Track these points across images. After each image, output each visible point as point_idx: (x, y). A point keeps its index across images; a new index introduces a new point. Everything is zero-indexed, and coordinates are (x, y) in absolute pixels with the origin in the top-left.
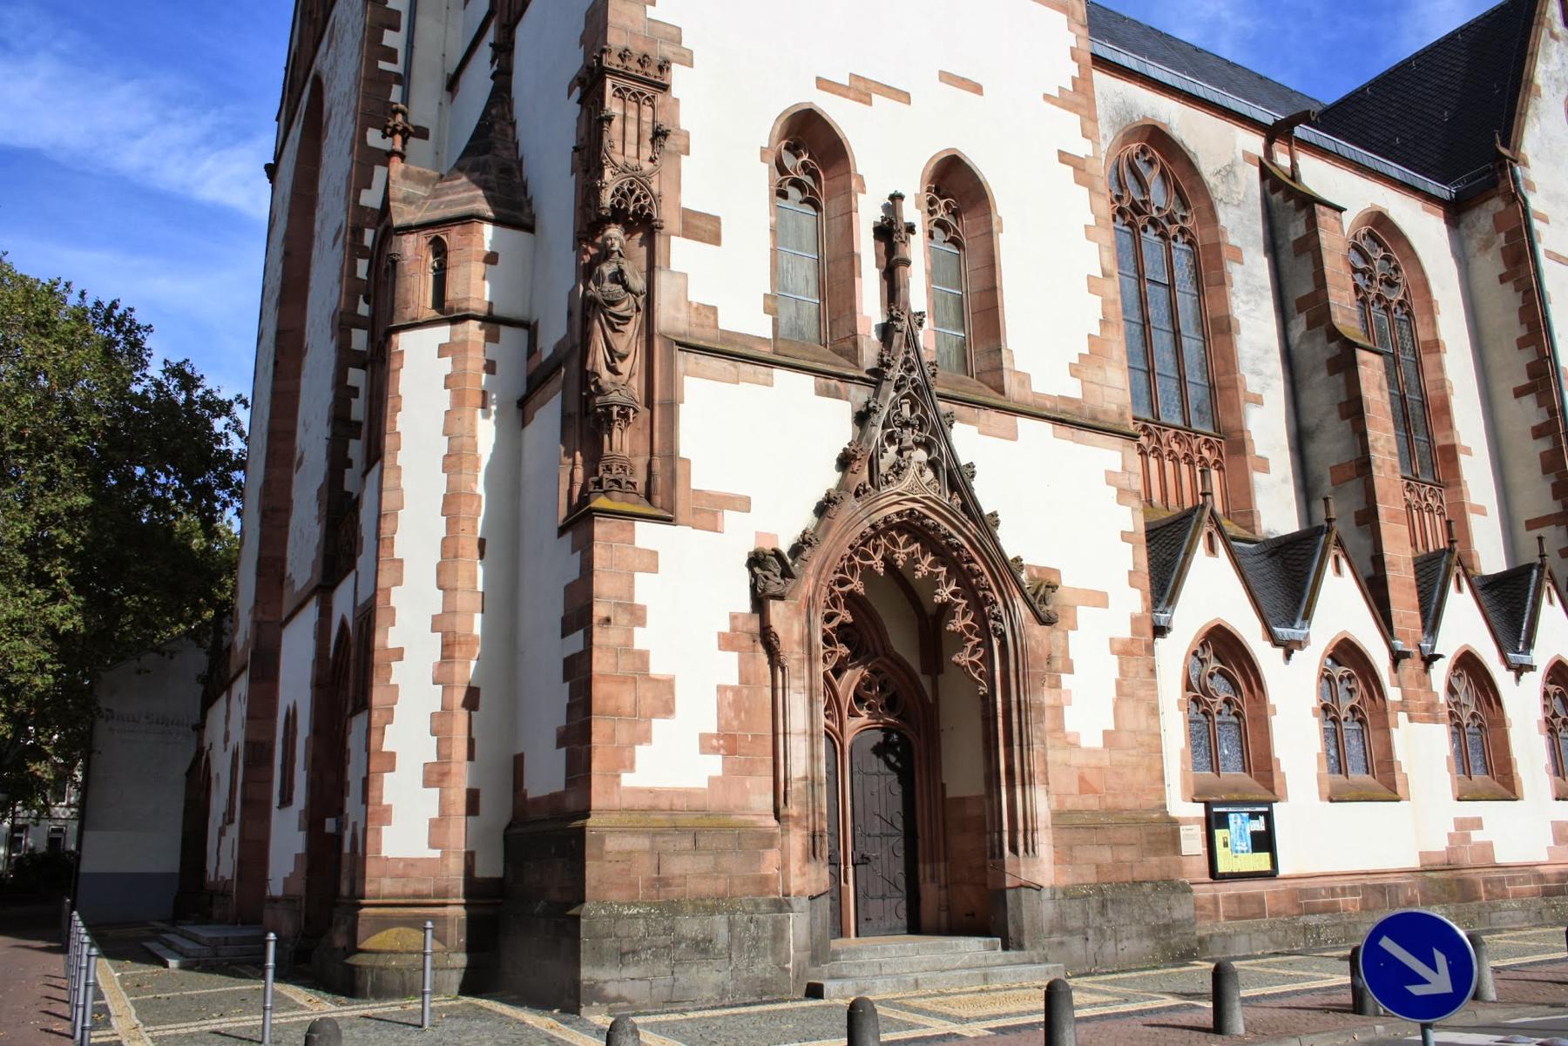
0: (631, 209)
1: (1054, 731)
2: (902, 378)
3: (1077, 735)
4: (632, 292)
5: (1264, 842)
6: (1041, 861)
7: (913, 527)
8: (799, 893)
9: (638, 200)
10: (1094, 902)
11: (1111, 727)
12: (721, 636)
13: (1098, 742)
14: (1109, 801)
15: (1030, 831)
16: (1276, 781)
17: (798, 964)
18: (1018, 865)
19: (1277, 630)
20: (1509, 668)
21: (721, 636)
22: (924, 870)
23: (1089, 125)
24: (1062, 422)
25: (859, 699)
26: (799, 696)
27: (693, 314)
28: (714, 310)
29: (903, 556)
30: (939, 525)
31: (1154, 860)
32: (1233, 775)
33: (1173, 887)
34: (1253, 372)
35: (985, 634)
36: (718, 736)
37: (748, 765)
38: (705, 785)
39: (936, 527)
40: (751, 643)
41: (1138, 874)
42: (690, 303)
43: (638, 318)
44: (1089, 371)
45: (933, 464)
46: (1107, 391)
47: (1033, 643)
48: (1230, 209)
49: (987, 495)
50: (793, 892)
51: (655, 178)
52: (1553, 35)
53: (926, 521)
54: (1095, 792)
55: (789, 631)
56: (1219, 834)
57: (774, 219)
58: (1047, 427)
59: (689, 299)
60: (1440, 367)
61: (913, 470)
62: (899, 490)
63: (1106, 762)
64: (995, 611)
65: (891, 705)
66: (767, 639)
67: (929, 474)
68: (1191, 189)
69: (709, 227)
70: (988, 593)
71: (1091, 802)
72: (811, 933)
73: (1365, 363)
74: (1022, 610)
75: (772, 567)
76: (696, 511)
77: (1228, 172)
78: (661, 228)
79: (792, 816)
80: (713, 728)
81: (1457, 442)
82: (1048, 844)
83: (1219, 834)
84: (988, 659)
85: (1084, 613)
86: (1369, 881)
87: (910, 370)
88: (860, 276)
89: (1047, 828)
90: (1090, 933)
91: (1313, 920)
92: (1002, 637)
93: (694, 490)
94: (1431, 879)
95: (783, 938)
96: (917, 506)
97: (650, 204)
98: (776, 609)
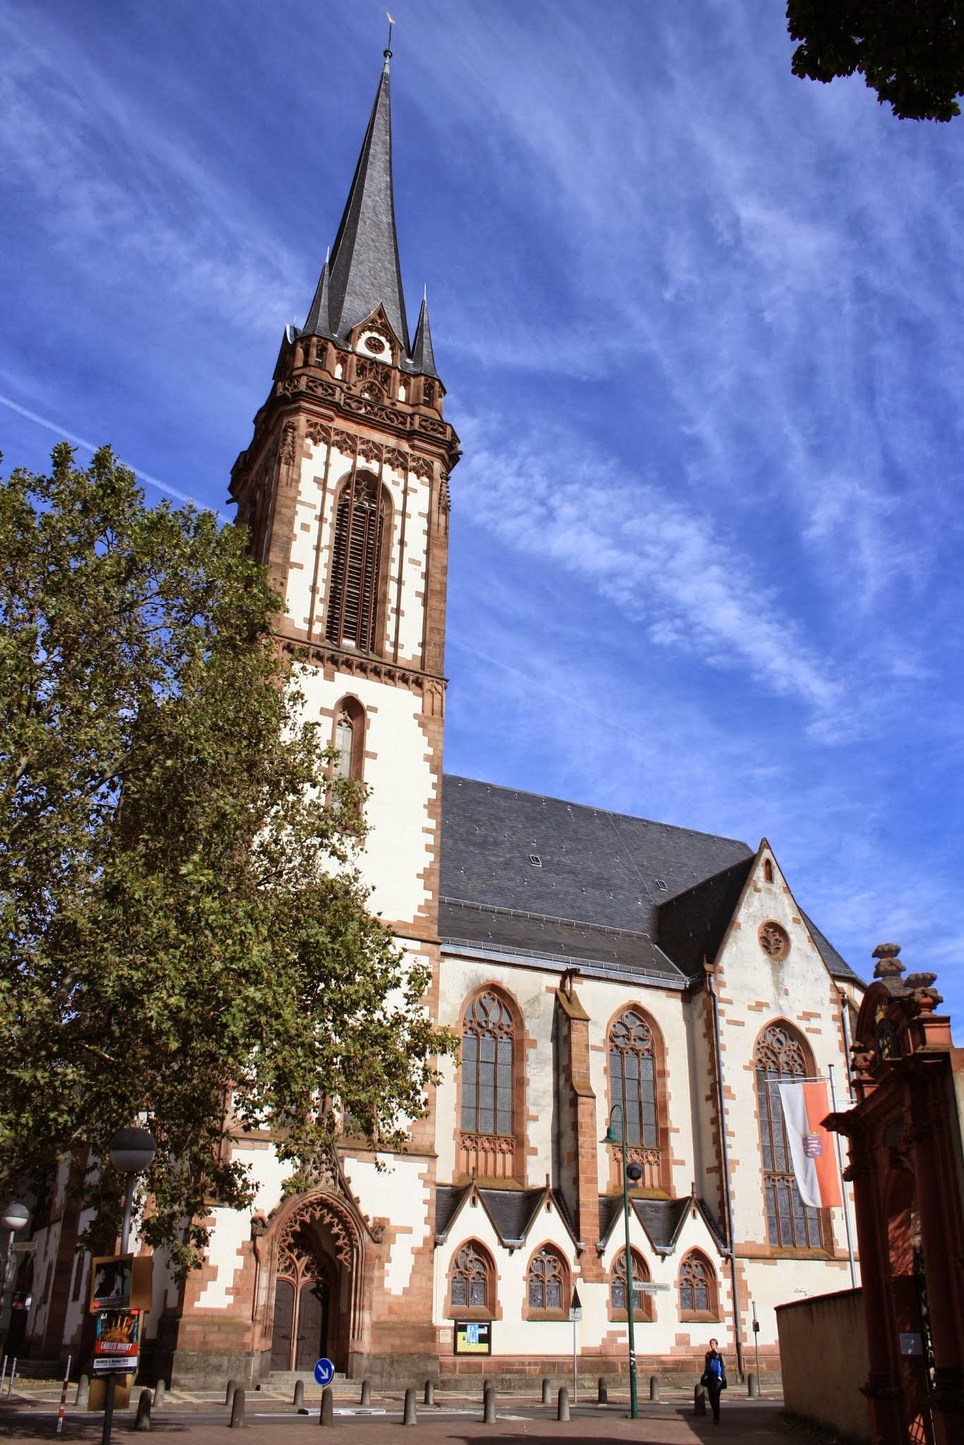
5: (485, 1339)
7: (322, 1203)
10: (388, 1361)
11: (407, 1285)
13: (400, 1292)
15: (361, 1329)
16: (497, 1311)
17: (254, 1378)
19: (505, 1240)
20: (657, 1254)
22: (329, 1344)
23: (433, 1011)
25: (307, 1268)
31: (421, 1345)
32: (478, 1307)
33: (429, 1356)
34: (534, 1105)
35: (352, 1246)
41: (412, 1350)
45: (333, 1177)
46: (425, 1136)
48: (533, 1020)
49: (355, 1190)
52: (757, 890)
55: (263, 1248)
56: (460, 1335)
60: (664, 1085)
61: (324, 1181)
63: (403, 1300)
65: (321, 1272)
66: (255, 1251)
67: (332, 1181)
68: (513, 1012)
71: (394, 1318)
73: (583, 1104)
74: (367, 1238)
77: (536, 999)
81: (669, 1126)
83: (460, 1335)
84: (352, 1257)
85: (398, 1236)
86: (545, 1359)
90: (385, 1374)
91: (508, 1376)
92: (358, 1248)
94: (587, 1362)
98: (259, 1240)
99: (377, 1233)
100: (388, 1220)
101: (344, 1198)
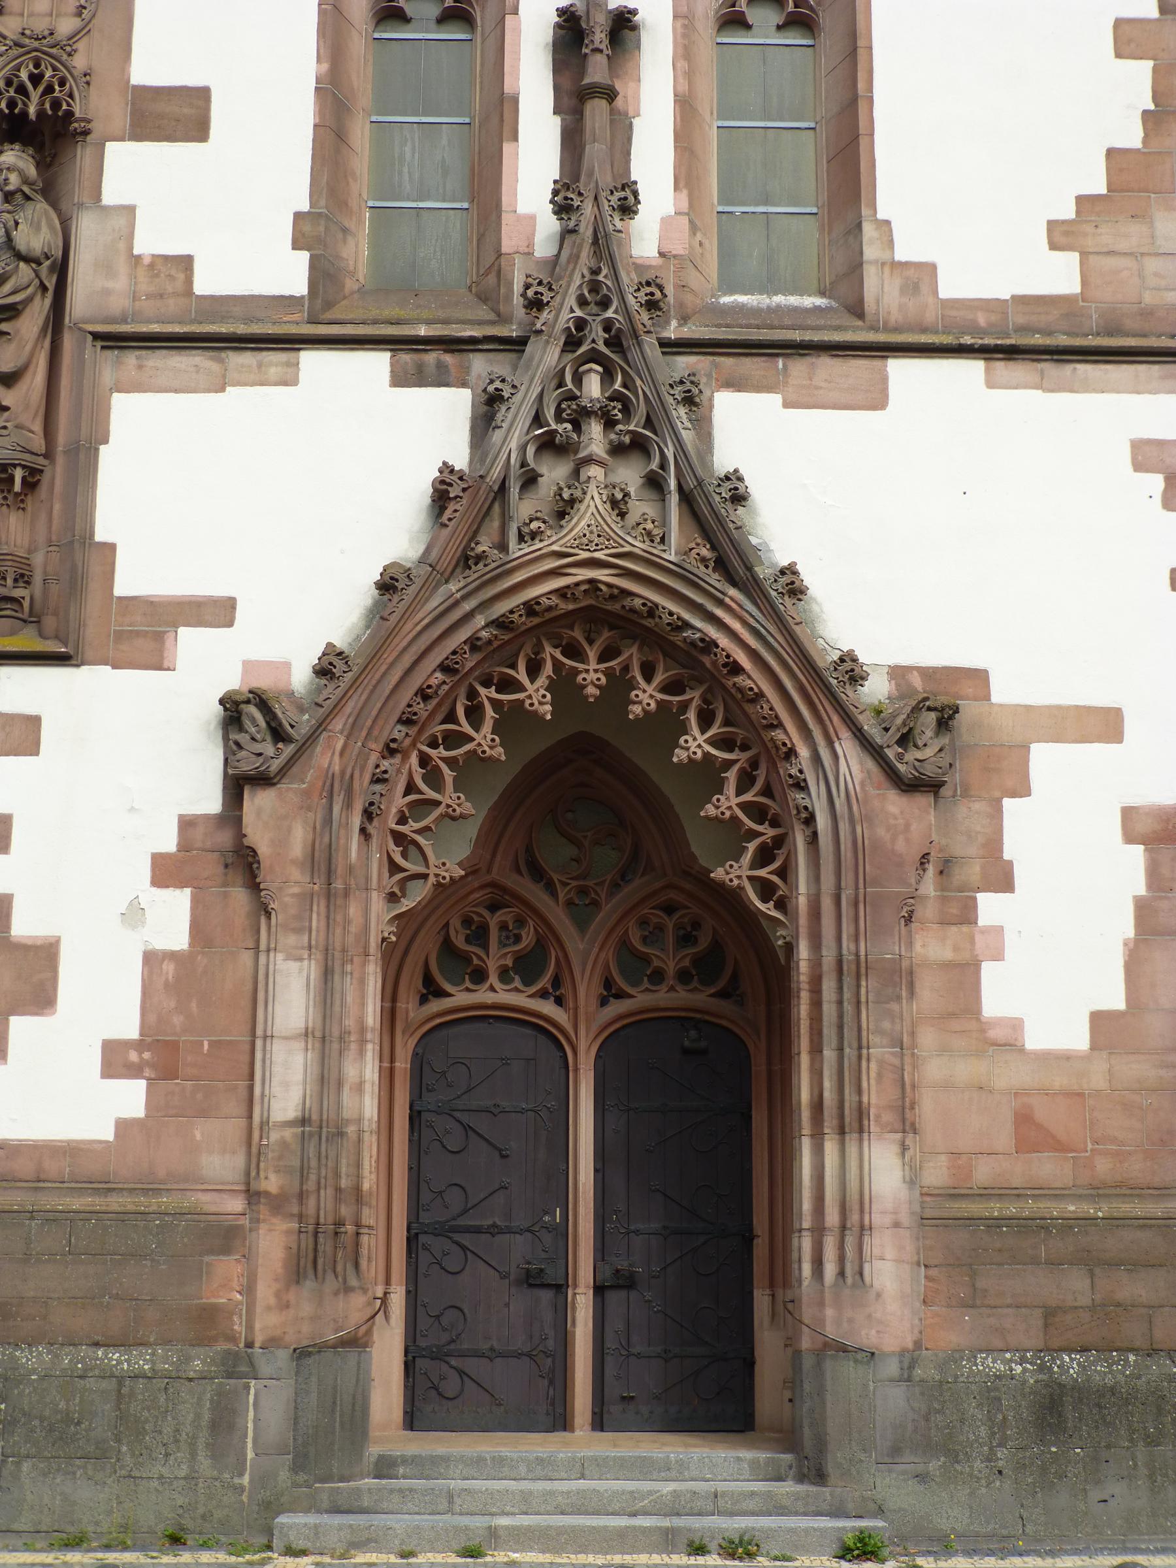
0: (32, 110)
1: (952, 1015)
2: (581, 324)
3: (1017, 1025)
4: (27, 259)
6: (878, 1295)
8: (272, 1343)
9: (49, 89)
11: (1118, 1003)
12: (158, 861)
13: (1079, 1039)
14: (1103, 1167)
18: (821, 1304)
21: (158, 861)
24: (1011, 353)
26: (293, 966)
27: (141, 274)
28: (186, 263)
29: (592, 676)
30: (657, 606)
36: (139, 1045)
37: (199, 1096)
38: (108, 1135)
39: (652, 610)
40: (221, 869)
42: (139, 258)
43: (39, 309)
44: (1103, 229)
47: (881, 832)
50: (259, 1340)
51: (81, 46)
53: (627, 602)
54: (1060, 1147)
57: (325, 66)
58: (973, 369)
59: (136, 252)
62: (555, 548)
63: (1097, 1079)
64: (794, 771)
69: (186, 111)
70: (779, 735)
72: (296, 1423)
75: (247, 723)
76: (120, 636)
78: (86, 133)
79: (267, 1194)
80: (130, 1030)
82: (898, 1261)
87: (605, 304)
88: (515, 138)
89: (897, 1225)
92: (810, 820)
93: (120, 598)
95: (231, 1427)
96: (601, 575)
97: (71, 96)
99: (905, 740)
100: (979, 677)
101: (714, 579)
